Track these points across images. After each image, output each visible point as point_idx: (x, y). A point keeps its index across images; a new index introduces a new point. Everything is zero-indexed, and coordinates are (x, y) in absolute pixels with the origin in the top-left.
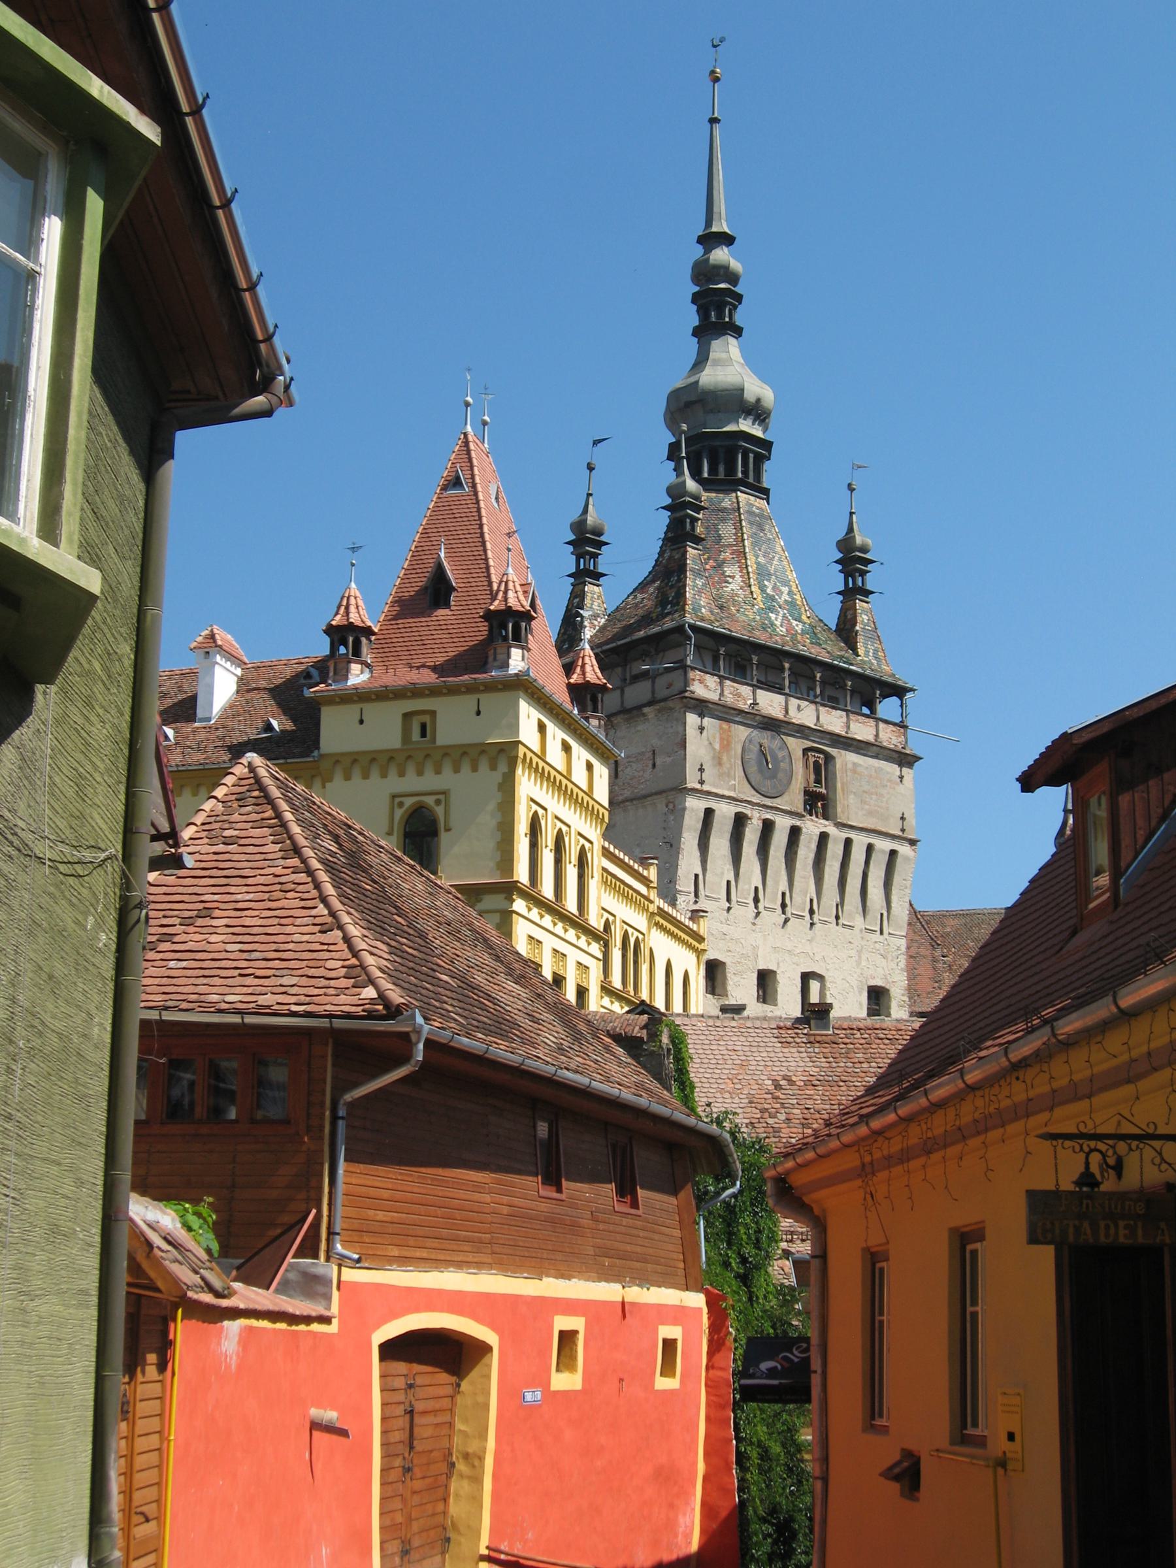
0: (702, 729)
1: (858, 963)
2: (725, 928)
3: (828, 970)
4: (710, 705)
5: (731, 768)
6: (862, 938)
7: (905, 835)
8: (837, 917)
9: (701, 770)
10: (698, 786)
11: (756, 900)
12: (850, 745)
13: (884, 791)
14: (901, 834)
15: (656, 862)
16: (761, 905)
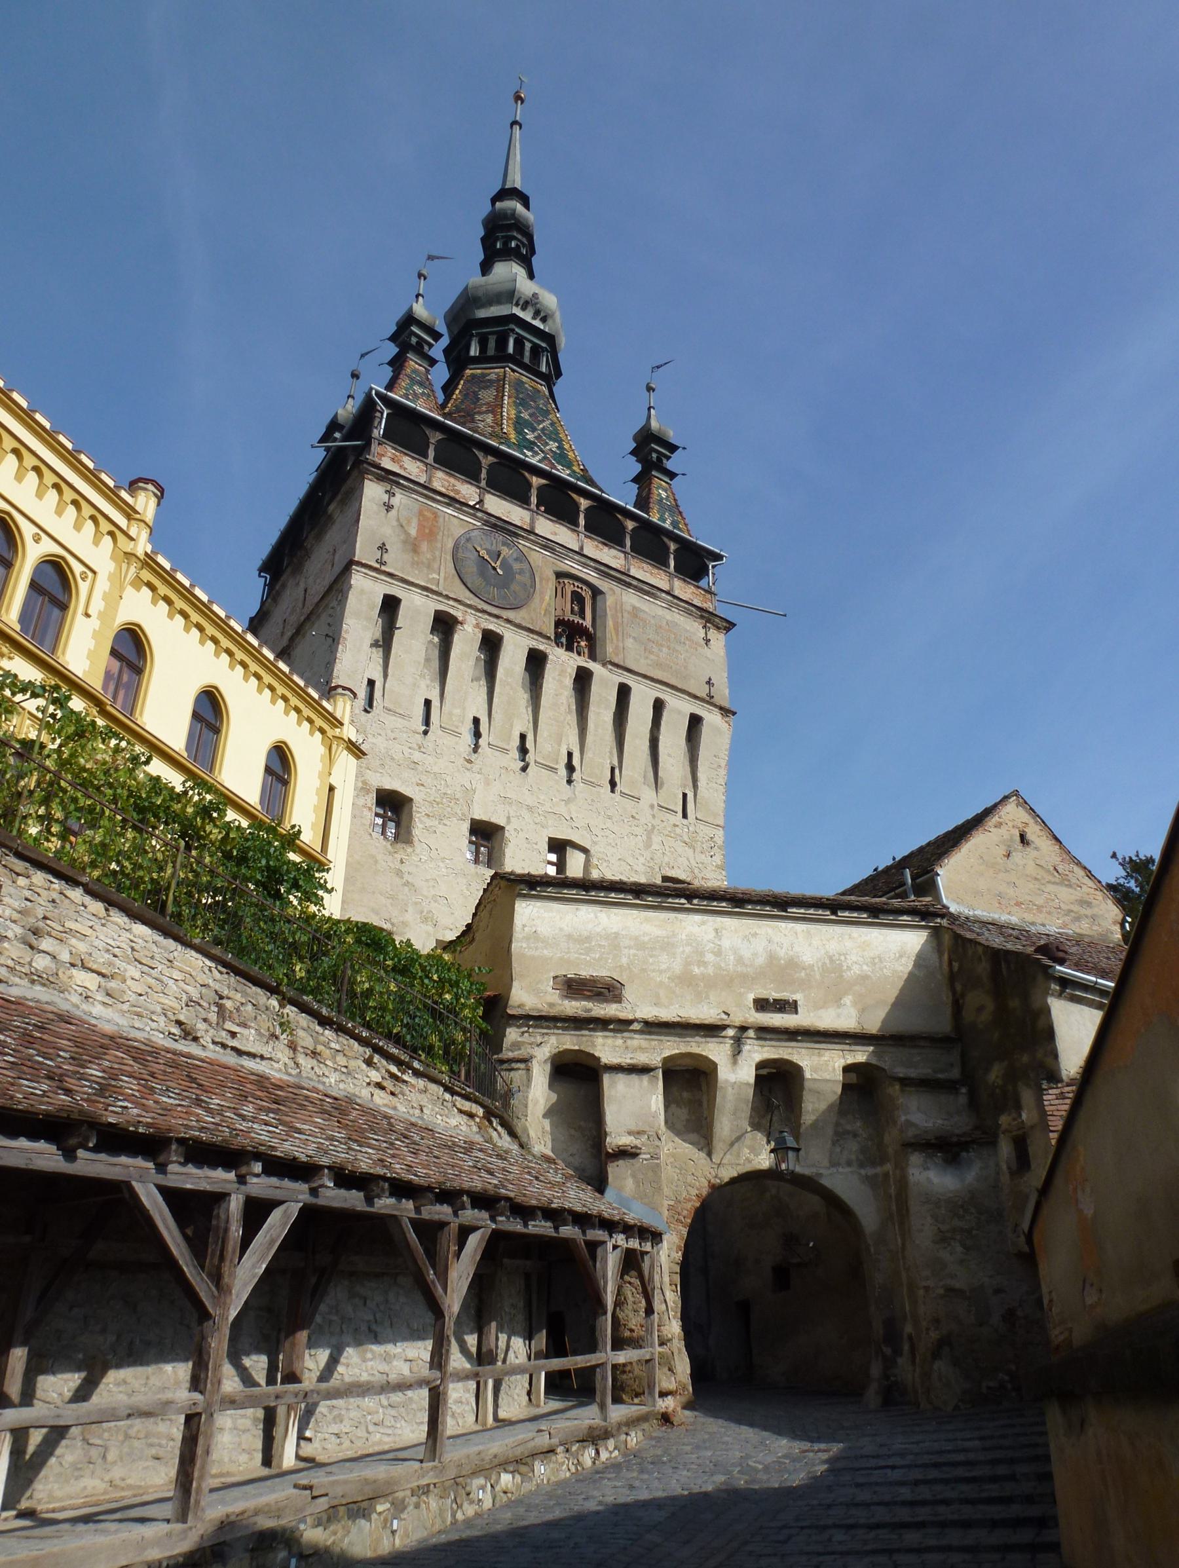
0: (389, 507)
1: (648, 845)
2: (417, 756)
3: (595, 843)
4: (401, 481)
5: (434, 559)
6: (654, 816)
7: (714, 700)
8: (613, 784)
9: (382, 548)
10: (377, 566)
11: (477, 735)
12: (629, 585)
13: (679, 648)
14: (708, 698)
15: (150, 487)
16: (482, 742)
